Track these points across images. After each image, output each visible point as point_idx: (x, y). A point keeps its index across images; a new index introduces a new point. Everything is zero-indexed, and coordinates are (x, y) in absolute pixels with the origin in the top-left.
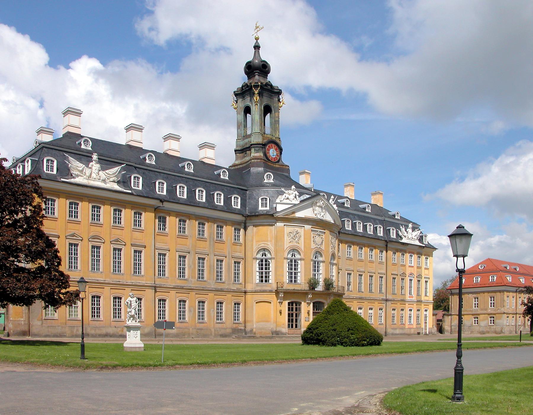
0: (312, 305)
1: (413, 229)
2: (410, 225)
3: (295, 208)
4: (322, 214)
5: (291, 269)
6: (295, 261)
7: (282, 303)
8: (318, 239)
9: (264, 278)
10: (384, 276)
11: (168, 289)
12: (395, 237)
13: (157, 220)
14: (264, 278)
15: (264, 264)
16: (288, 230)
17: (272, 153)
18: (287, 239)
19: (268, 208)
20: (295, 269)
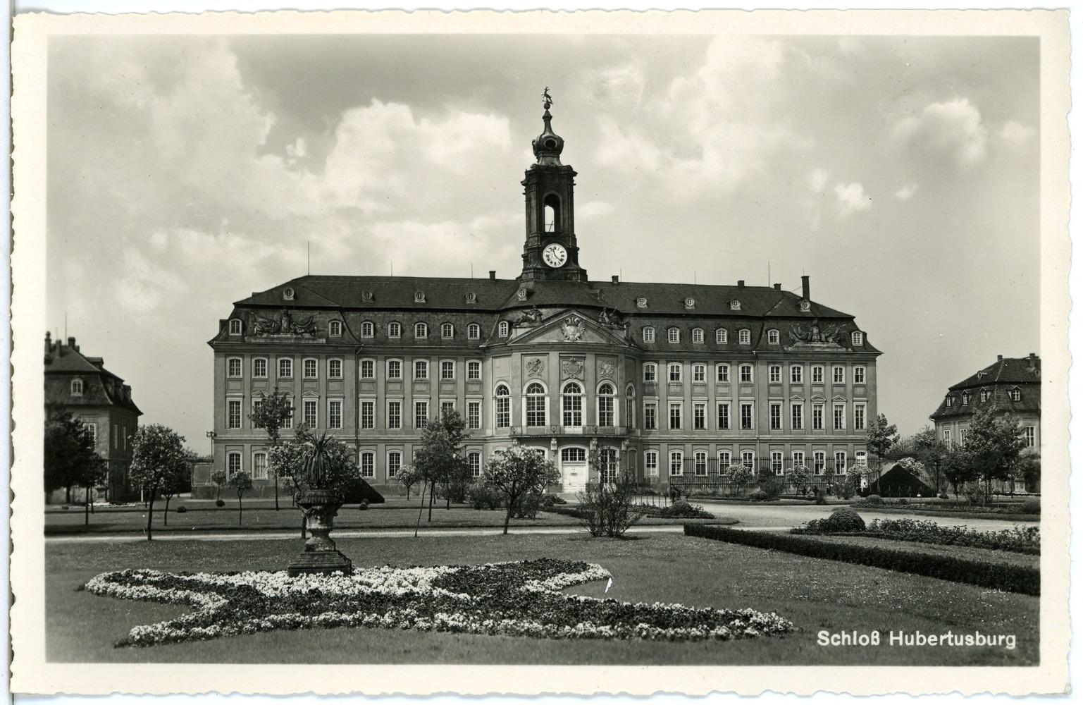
11: (375, 442)
15: (504, 405)
16: (528, 359)
18: (526, 372)
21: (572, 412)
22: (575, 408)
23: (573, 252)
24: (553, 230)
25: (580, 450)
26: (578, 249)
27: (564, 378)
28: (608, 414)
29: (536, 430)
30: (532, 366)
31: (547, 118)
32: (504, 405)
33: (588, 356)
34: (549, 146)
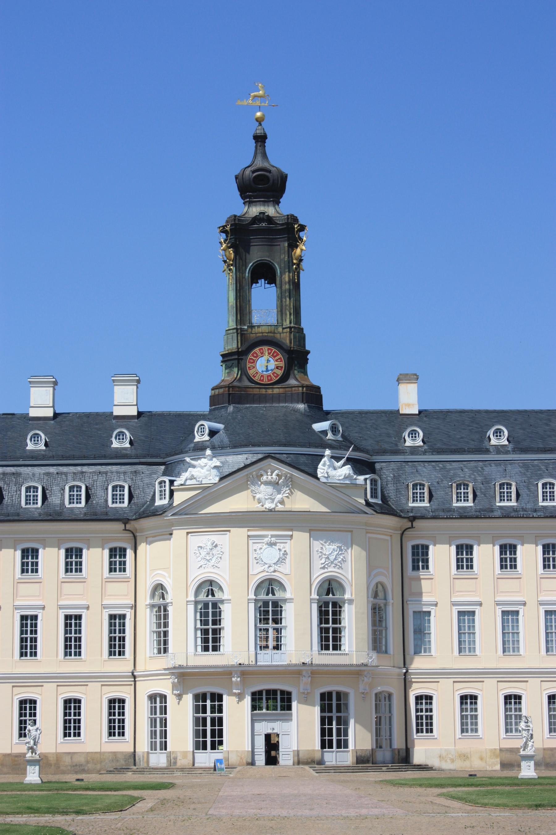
3: (208, 494)
4: (279, 497)
5: (206, 623)
6: (215, 605)
7: (179, 697)
8: (271, 555)
17: (265, 364)
18: (194, 562)
19: (166, 502)
20: (215, 623)
22: (276, 621)
23: (296, 358)
24: (272, 319)
25: (282, 692)
26: (308, 352)
27: (256, 572)
28: (335, 630)
29: (210, 659)
30: (203, 553)
32: (162, 613)
33: (296, 534)
34: (263, 185)
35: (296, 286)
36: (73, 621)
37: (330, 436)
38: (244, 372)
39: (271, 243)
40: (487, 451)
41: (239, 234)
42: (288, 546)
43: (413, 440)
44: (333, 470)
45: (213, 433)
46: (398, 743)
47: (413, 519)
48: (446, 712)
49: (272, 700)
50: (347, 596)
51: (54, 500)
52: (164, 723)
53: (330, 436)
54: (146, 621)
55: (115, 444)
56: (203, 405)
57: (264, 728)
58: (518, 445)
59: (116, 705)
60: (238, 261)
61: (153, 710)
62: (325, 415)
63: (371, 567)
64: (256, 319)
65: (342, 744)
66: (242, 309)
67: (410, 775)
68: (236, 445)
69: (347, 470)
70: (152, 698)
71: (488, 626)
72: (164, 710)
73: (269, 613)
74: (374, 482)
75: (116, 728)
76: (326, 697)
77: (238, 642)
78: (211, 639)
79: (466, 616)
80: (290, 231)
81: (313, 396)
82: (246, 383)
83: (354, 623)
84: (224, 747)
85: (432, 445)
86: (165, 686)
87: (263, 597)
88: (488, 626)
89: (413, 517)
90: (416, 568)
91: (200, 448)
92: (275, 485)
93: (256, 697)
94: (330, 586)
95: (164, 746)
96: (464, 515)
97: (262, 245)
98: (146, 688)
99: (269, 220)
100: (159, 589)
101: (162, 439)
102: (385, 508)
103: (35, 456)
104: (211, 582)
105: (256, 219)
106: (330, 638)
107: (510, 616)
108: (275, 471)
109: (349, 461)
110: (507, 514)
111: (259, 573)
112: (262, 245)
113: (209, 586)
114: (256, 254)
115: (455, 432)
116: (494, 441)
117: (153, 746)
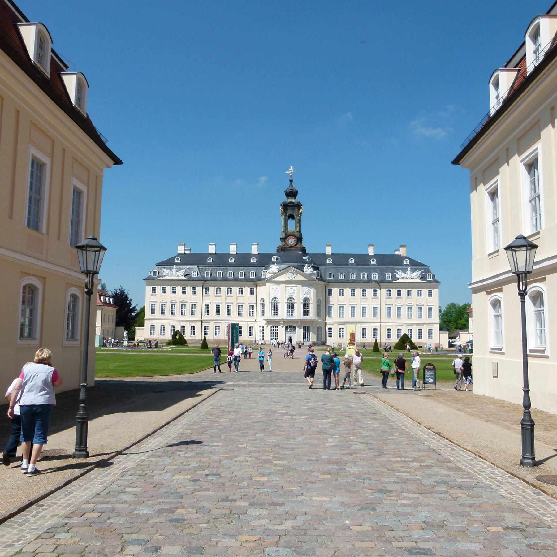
0: (285, 327)
1: (413, 271)
2: (409, 269)
3: (276, 275)
8: (291, 291)
9: (263, 314)
10: (378, 307)
12: (390, 279)
13: (204, 290)
14: (263, 314)
17: (291, 241)
21: (291, 309)
23: (299, 240)
31: (291, 181)
32: (263, 305)
34: (292, 194)
35: (300, 221)
36: (240, 307)
37: (307, 260)
38: (286, 243)
39: (293, 209)
40: (348, 265)
41: (285, 206)
42: (295, 289)
43: (329, 261)
44: (308, 270)
45: (277, 259)
46: (323, 340)
47: (328, 282)
48: (335, 333)
49: (290, 327)
50: (310, 302)
51: (236, 275)
52: (263, 333)
53: (307, 260)
54: (259, 308)
55: (252, 261)
56: (275, 252)
57: (289, 335)
58: (357, 263)
59: (251, 328)
60: (285, 214)
61: (260, 330)
62: (307, 255)
63: (317, 295)
64: (289, 229)
65: (308, 340)
66: (286, 226)
67: (325, 347)
68: (283, 262)
69: (311, 269)
70: (260, 327)
71: (347, 311)
72: (263, 330)
73: (290, 306)
74: (318, 273)
75: (251, 334)
76: (304, 328)
77: (282, 314)
78: (275, 312)
79: (341, 308)
80: (298, 206)
81: (303, 250)
82: (286, 246)
83: (312, 309)
84: (278, 340)
85: (334, 263)
86: (264, 324)
87: (289, 302)
88: (347, 311)
89: (329, 282)
90: (329, 295)
91: (274, 263)
92: (293, 273)
93: (287, 327)
94: (306, 299)
95: (263, 339)
96: (342, 281)
97: (291, 210)
98: (259, 324)
99: (293, 203)
100: (262, 299)
101: (264, 260)
102: (321, 279)
103: (231, 264)
104: (276, 298)
105: (290, 203)
106: (306, 313)
107: (353, 308)
108: (293, 270)
109: (312, 267)
110: (353, 281)
111: (288, 296)
112: (291, 210)
113: (275, 299)
114: (289, 212)
115: (340, 259)
116: (350, 262)
117: (260, 339)
